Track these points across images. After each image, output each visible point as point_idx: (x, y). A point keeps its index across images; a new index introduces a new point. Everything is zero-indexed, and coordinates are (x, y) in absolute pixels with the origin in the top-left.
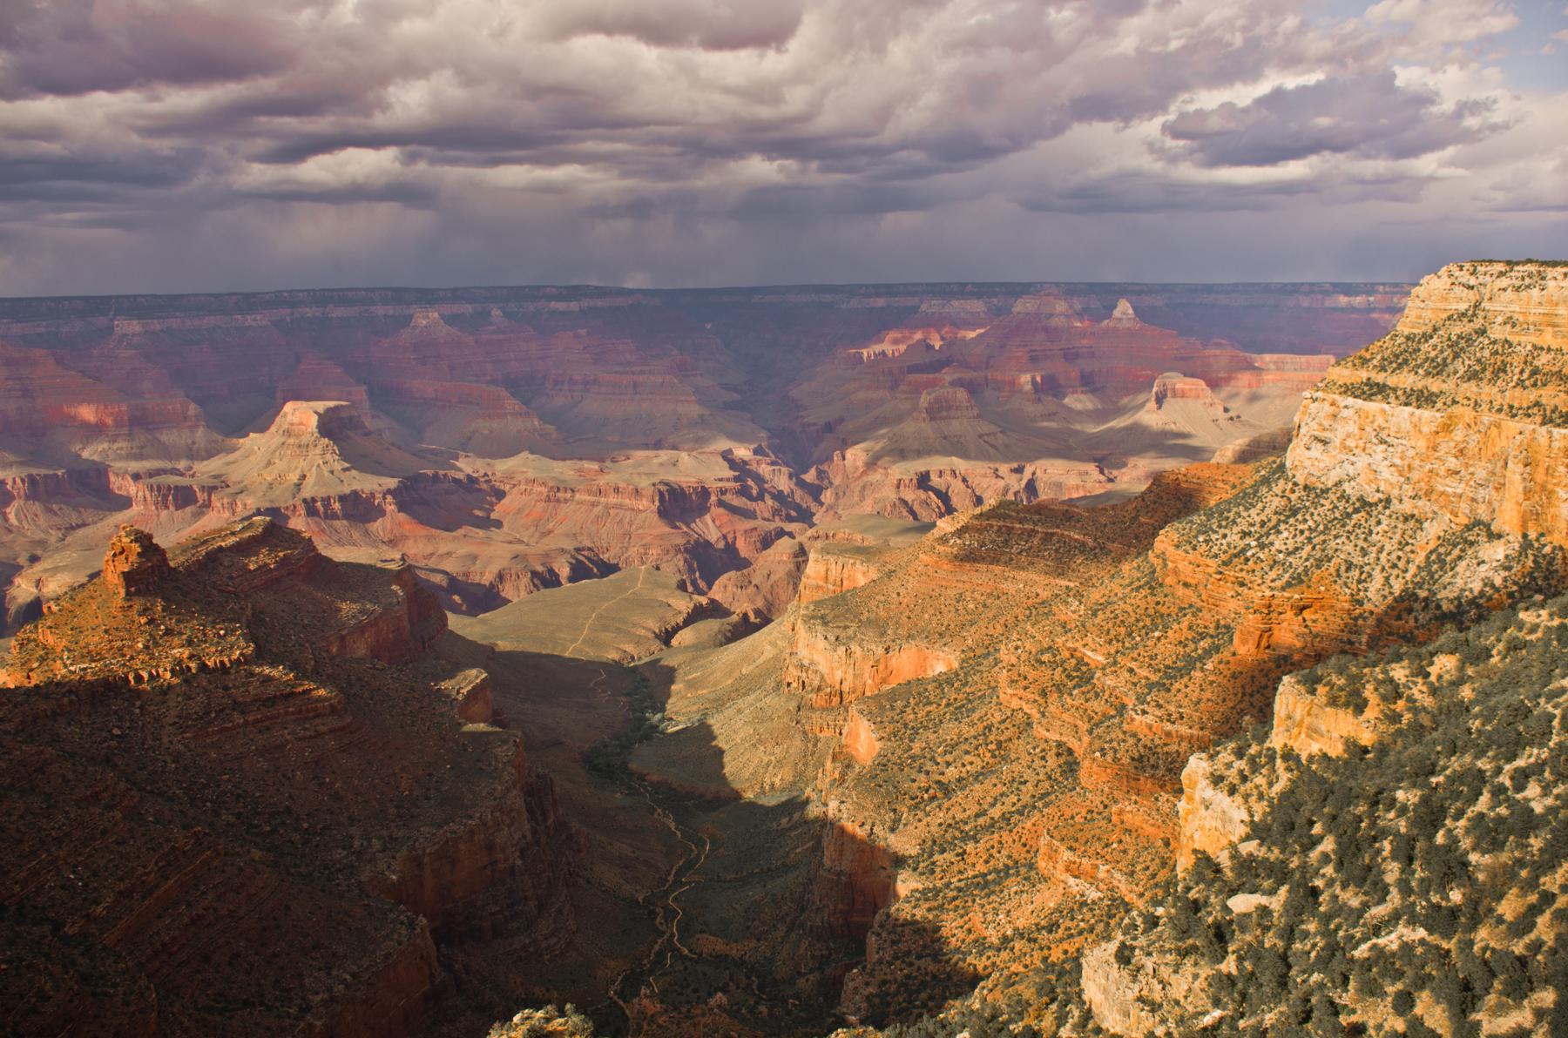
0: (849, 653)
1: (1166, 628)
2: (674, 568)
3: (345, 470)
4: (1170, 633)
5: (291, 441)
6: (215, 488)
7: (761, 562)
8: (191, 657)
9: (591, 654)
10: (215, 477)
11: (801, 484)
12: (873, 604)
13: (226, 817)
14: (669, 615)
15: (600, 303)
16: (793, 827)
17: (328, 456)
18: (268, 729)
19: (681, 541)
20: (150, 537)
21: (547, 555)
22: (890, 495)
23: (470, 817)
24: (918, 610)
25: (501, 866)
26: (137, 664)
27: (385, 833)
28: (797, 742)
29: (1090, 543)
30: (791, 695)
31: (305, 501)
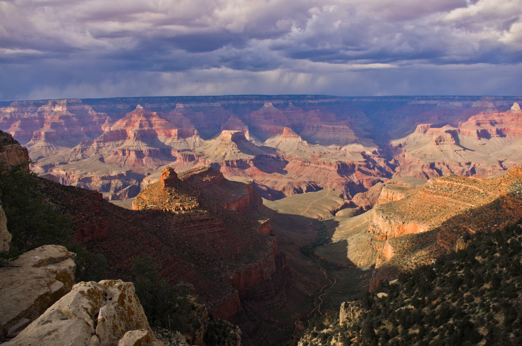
0: (390, 223)
1: (500, 223)
2: (341, 190)
3: (238, 152)
4: (501, 225)
5: (223, 142)
6: (200, 156)
7: (370, 190)
8: (181, 206)
9: (308, 216)
10: (201, 152)
11: (388, 164)
12: (400, 207)
13: (186, 254)
15: (325, 101)
16: (364, 279)
17: (234, 148)
19: (344, 181)
20: (173, 170)
22: (419, 170)
23: (256, 262)
24: (416, 210)
25: (265, 278)
26: (166, 206)
27: (230, 264)
28: (370, 251)
29: (482, 191)
30: (370, 235)
31: (226, 161)
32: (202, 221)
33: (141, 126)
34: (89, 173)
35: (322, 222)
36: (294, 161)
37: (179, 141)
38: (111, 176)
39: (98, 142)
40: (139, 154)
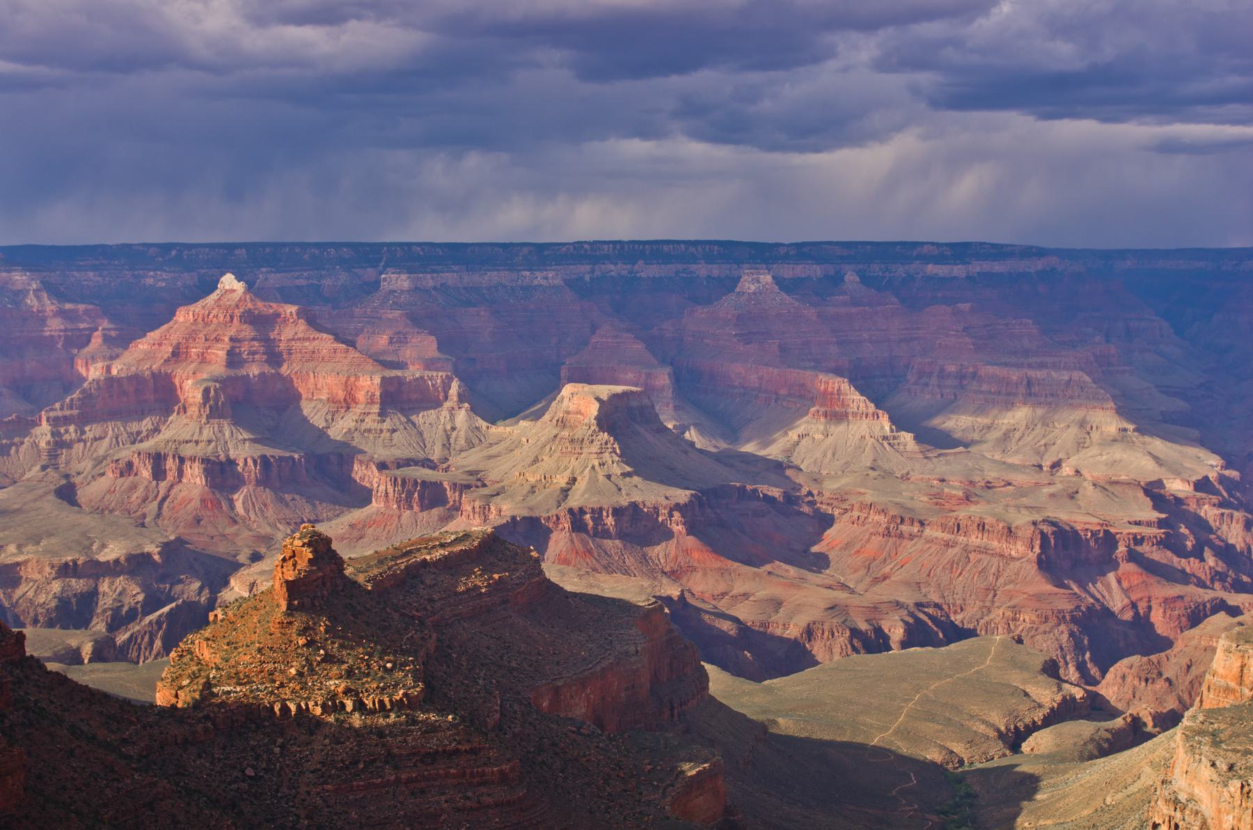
2: (1052, 641)
3: (625, 475)
5: (565, 433)
6: (468, 487)
7: (1179, 646)
8: (347, 691)
9: (904, 748)
10: (471, 473)
14: (1023, 708)
15: (998, 267)
18: (422, 792)
19: (1067, 606)
26: (286, 693)
31: (571, 511)
32: (433, 757)
33: (233, 359)
34: (12, 548)
35: (960, 779)
36: (856, 513)
37: (387, 425)
38: (98, 563)
39: (55, 422)
40: (222, 474)
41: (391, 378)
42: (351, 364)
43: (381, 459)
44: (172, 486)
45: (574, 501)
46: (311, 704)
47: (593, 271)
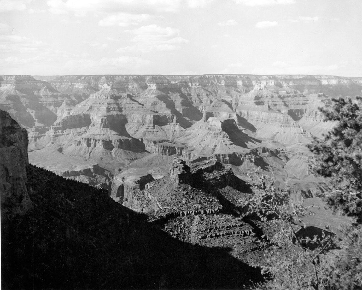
3: (231, 144)
5: (211, 132)
8: (201, 208)
10: (183, 144)
21: (307, 184)
31: (216, 155)
33: (108, 110)
36: (298, 156)
37: (155, 130)
40: (108, 145)
41: (156, 116)
42: (144, 111)
43: (155, 140)
44: (93, 148)
45: (217, 152)
46: (191, 212)
47: (209, 83)
